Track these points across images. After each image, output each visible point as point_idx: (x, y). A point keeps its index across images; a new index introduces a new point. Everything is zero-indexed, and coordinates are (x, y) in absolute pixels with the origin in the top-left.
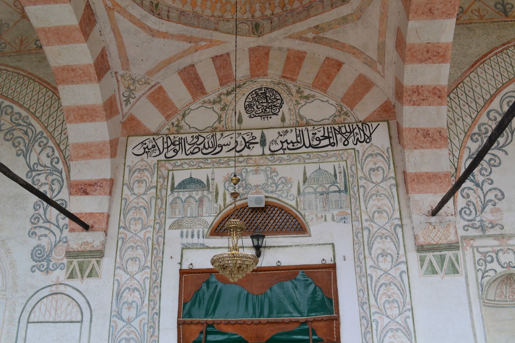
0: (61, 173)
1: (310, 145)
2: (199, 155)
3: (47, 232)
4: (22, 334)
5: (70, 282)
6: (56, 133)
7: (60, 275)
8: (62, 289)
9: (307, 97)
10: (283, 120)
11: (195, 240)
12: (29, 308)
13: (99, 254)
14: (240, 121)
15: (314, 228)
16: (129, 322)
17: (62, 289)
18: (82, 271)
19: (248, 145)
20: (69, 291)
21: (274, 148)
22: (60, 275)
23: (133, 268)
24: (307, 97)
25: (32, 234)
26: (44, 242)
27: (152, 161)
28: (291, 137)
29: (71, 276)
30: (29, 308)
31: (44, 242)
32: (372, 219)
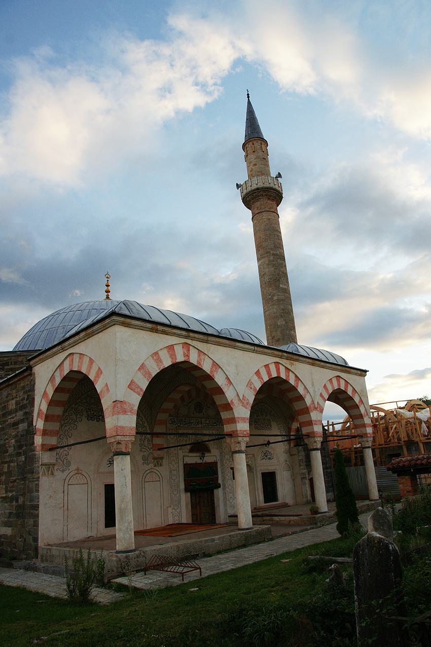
0: (146, 427)
1: (212, 425)
2: (186, 426)
3: (145, 450)
4: (143, 486)
5: (155, 468)
6: (144, 411)
7: (151, 465)
8: (153, 470)
9: (209, 407)
10: (203, 414)
11: (186, 454)
12: (144, 477)
13: (162, 458)
14: (193, 414)
15: (212, 451)
16: (174, 480)
17: (153, 470)
18: (158, 464)
19: (198, 423)
20: (155, 471)
21: (204, 425)
22: (151, 465)
23: (173, 463)
24: (209, 407)
25: (141, 451)
26: (145, 454)
27: (175, 426)
28: (207, 422)
29: (155, 466)
30: (144, 477)
31: (145, 454)
32: (225, 449)
